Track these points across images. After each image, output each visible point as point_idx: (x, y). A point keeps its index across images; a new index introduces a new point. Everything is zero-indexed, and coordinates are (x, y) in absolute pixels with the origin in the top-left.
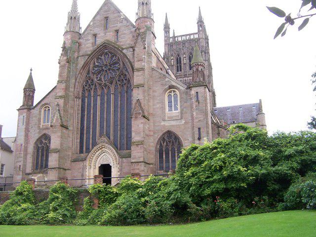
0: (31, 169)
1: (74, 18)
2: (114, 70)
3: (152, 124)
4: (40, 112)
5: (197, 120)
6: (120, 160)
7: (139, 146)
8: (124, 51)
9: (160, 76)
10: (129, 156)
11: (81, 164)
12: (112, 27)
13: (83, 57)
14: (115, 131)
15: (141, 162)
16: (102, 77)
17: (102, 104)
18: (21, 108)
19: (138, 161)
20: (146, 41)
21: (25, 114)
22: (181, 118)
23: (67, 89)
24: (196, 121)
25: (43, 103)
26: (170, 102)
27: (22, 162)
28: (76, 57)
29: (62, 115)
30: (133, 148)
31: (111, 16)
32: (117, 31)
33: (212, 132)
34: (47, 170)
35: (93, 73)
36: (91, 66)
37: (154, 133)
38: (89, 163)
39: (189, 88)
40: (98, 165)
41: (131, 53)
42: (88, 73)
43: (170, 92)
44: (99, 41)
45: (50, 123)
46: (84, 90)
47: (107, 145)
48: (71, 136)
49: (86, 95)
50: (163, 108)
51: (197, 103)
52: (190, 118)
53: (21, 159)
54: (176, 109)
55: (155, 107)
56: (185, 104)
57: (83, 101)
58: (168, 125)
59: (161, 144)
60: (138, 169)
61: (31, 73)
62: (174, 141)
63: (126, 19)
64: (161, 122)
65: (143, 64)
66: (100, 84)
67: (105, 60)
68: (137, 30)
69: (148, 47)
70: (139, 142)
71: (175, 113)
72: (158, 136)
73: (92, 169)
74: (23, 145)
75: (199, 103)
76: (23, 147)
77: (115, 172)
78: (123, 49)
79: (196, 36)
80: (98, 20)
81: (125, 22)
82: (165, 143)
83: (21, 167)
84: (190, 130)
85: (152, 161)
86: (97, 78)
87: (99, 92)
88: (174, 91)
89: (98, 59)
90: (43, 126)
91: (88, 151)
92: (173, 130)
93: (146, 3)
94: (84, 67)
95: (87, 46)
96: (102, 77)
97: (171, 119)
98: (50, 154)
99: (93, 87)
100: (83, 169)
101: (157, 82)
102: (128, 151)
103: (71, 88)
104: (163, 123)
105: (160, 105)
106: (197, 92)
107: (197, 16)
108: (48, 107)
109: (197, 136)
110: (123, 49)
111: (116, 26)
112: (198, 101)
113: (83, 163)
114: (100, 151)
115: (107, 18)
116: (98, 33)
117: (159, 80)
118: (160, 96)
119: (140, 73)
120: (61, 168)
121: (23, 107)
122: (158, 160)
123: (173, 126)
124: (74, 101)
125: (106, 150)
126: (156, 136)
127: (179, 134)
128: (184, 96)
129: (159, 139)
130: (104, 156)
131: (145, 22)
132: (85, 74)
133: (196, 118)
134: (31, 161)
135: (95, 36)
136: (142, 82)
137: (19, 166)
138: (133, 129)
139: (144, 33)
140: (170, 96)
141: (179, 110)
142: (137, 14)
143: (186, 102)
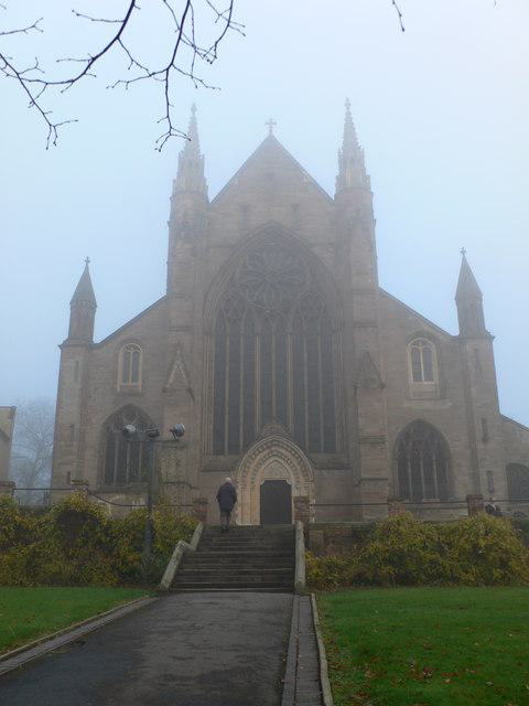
1: (191, 165)
6: (317, 472)
27: (75, 465)
40: (259, 482)
45: (140, 383)
54: (429, 377)
73: (249, 487)
74: (77, 426)
90: (121, 387)
104: (406, 405)
125: (281, 450)
137: (66, 474)
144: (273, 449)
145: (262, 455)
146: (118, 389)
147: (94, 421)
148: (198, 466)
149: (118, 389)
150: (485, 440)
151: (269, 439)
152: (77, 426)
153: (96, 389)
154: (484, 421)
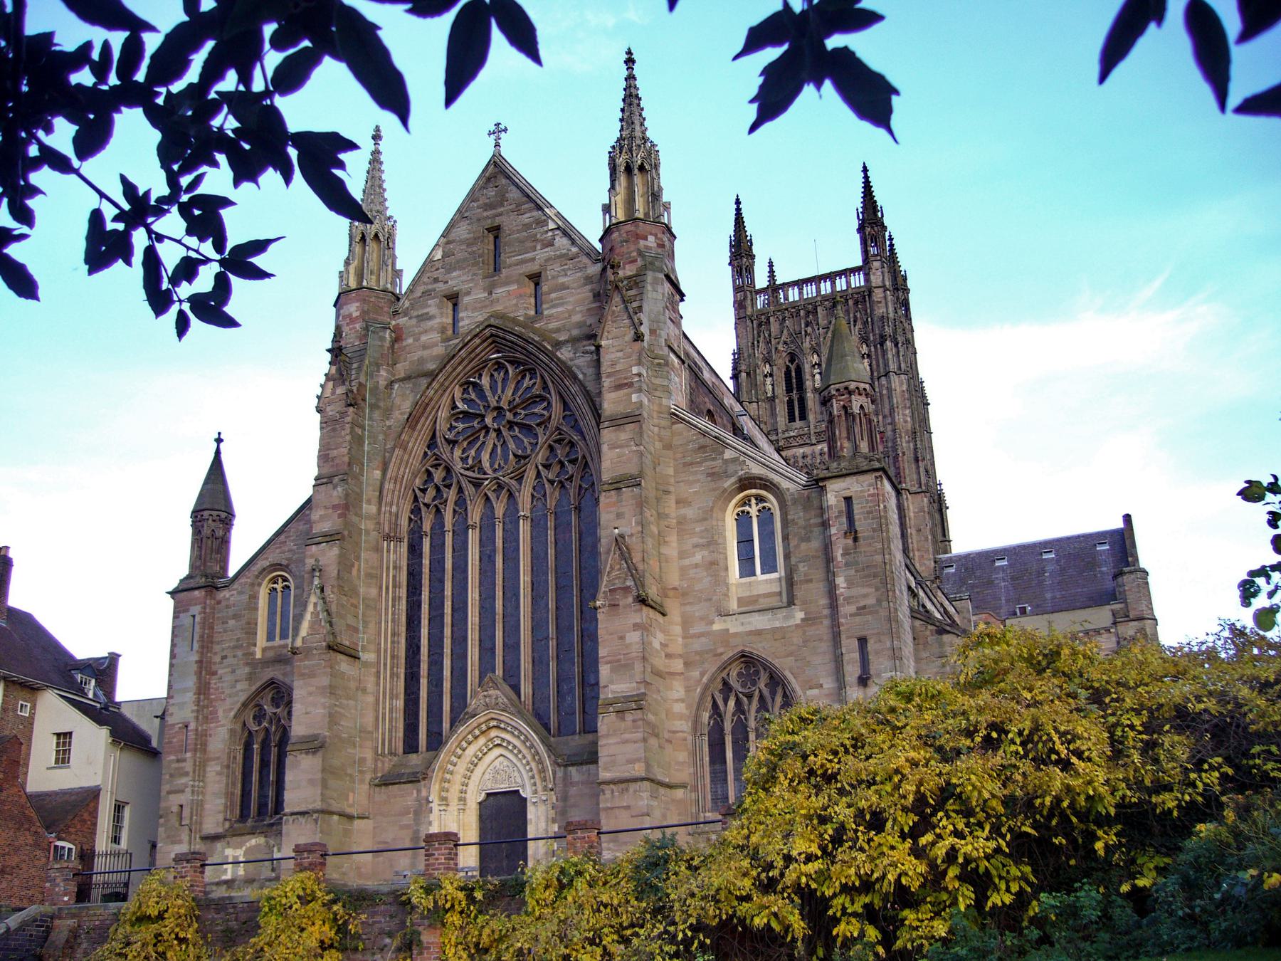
0: (221, 817)
2: (526, 428)
3: (677, 630)
4: (254, 597)
5: (852, 609)
6: (560, 773)
7: (629, 717)
8: (565, 354)
9: (702, 441)
10: (592, 758)
11: (406, 796)
12: (517, 262)
13: (409, 385)
14: (539, 662)
15: (635, 780)
16: (485, 457)
17: (487, 559)
18: (185, 587)
19: (627, 775)
20: (645, 308)
21: (196, 610)
22: (791, 602)
23: (348, 507)
24: (846, 610)
25: (263, 563)
26: (745, 542)
28: (382, 383)
29: (333, 608)
30: (605, 723)
31: (511, 223)
32: (536, 278)
33: (916, 650)
34: (279, 823)
35: (452, 443)
36: (443, 414)
37: (686, 664)
38: (443, 789)
39: (817, 481)
40: (475, 797)
41: (588, 358)
42: (432, 444)
43: (746, 502)
44: (470, 319)
46: (416, 511)
47: (505, 717)
48: (370, 686)
49: (427, 527)
50: (716, 566)
51: (850, 541)
52: (824, 601)
53: (184, 780)
55: (687, 562)
56: (804, 546)
57: (414, 550)
58: (740, 629)
59: (715, 705)
60: (628, 807)
61: (218, 452)
62: (766, 692)
63: (567, 231)
64: (712, 623)
65: (634, 398)
66: (477, 484)
67: (493, 388)
68: (609, 271)
69: (653, 332)
70: (627, 699)
71: (766, 582)
72: (702, 674)
75: (856, 539)
76: (192, 736)
77: (538, 820)
78: (558, 345)
79: (858, 281)
80: (462, 242)
81: (561, 242)
82: (732, 703)
83: (186, 812)
84: (825, 646)
85: (684, 775)
86: (464, 460)
87: (475, 514)
88: (760, 499)
89: (466, 385)
91: (436, 742)
92: (760, 649)
93: (642, 168)
94: (412, 421)
95: (423, 338)
96: (485, 457)
97: (750, 606)
98: (289, 760)
99: (452, 495)
100: (418, 813)
101: (691, 464)
102: (590, 737)
103: (369, 502)
105: (706, 553)
106: (848, 500)
107: (857, 201)
108: (285, 580)
109: (852, 671)
110: (558, 345)
111: (533, 259)
112: (852, 532)
113: (419, 791)
114: (482, 741)
115: (496, 230)
116: (464, 287)
117: (698, 457)
118: (705, 519)
119: (624, 435)
120: (332, 813)
121: (192, 583)
122: (707, 768)
123: (759, 633)
124: (378, 549)
125: (504, 735)
126: (696, 674)
127: (785, 666)
128: (797, 514)
129: (706, 688)
130: (497, 763)
131: (639, 237)
132: (418, 445)
133: (848, 600)
134: (223, 785)
135: (454, 299)
136: (632, 469)
137: (175, 809)
138: (602, 652)
139: (636, 281)
140: (743, 520)
141: (781, 572)
142: (607, 209)
143: (808, 540)
144: (493, 733)
145: (472, 750)
146: (259, 655)
147: (220, 713)
148: (368, 777)
149: (259, 655)
150: (863, 681)
151: (481, 718)
152: (192, 726)
153: (224, 657)
154: (863, 641)
